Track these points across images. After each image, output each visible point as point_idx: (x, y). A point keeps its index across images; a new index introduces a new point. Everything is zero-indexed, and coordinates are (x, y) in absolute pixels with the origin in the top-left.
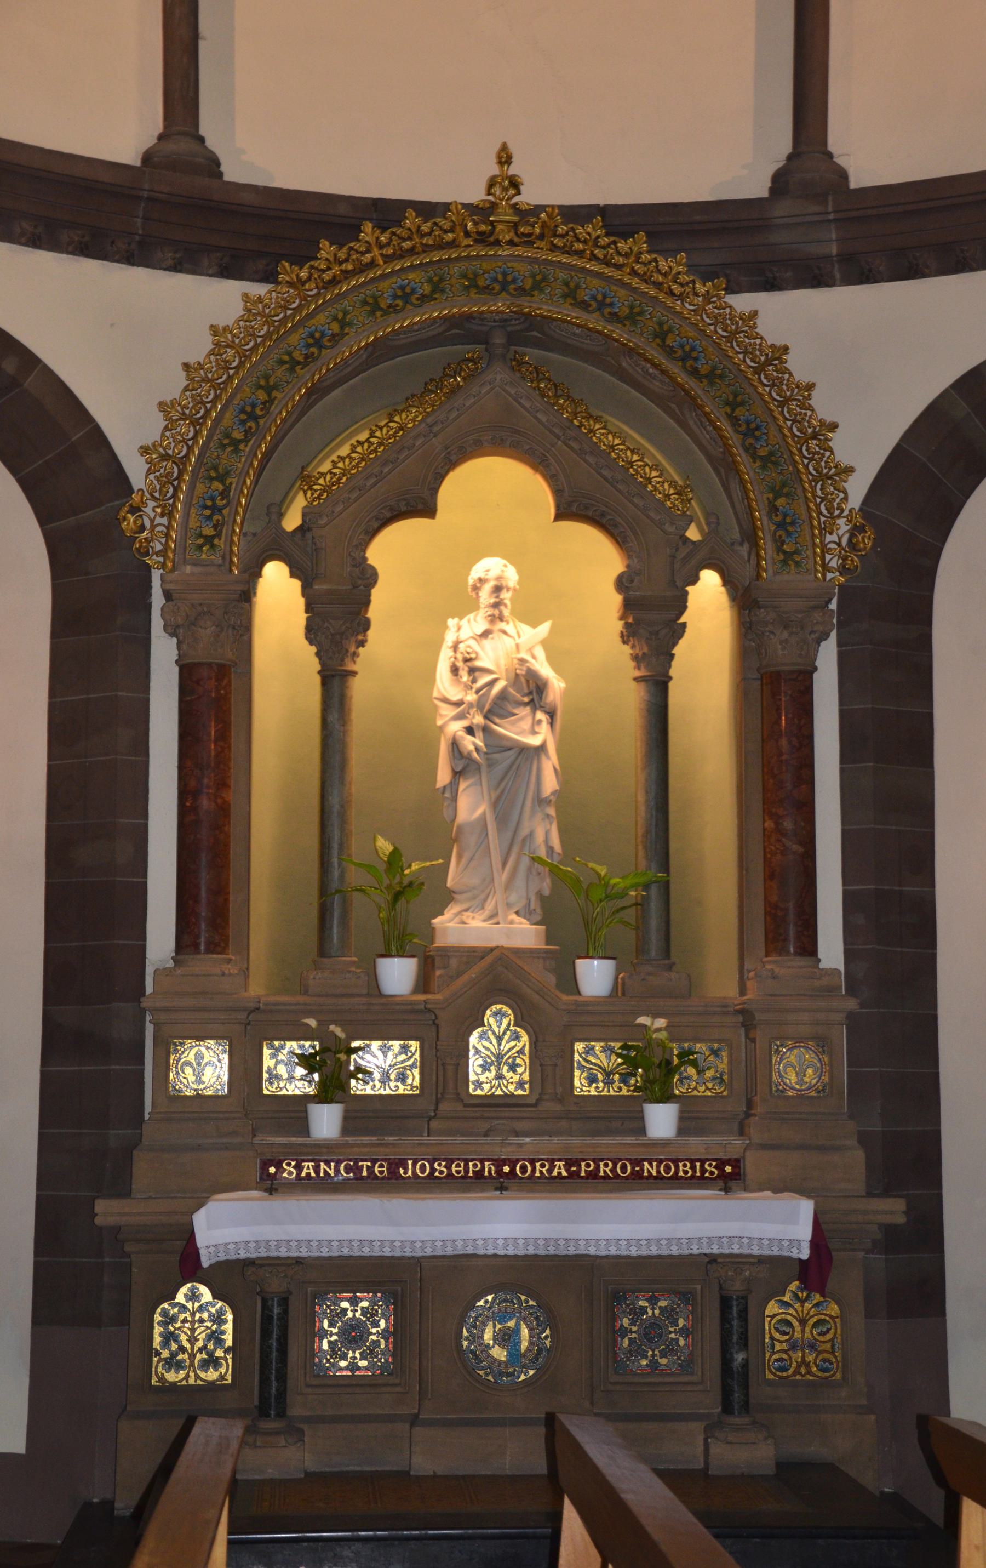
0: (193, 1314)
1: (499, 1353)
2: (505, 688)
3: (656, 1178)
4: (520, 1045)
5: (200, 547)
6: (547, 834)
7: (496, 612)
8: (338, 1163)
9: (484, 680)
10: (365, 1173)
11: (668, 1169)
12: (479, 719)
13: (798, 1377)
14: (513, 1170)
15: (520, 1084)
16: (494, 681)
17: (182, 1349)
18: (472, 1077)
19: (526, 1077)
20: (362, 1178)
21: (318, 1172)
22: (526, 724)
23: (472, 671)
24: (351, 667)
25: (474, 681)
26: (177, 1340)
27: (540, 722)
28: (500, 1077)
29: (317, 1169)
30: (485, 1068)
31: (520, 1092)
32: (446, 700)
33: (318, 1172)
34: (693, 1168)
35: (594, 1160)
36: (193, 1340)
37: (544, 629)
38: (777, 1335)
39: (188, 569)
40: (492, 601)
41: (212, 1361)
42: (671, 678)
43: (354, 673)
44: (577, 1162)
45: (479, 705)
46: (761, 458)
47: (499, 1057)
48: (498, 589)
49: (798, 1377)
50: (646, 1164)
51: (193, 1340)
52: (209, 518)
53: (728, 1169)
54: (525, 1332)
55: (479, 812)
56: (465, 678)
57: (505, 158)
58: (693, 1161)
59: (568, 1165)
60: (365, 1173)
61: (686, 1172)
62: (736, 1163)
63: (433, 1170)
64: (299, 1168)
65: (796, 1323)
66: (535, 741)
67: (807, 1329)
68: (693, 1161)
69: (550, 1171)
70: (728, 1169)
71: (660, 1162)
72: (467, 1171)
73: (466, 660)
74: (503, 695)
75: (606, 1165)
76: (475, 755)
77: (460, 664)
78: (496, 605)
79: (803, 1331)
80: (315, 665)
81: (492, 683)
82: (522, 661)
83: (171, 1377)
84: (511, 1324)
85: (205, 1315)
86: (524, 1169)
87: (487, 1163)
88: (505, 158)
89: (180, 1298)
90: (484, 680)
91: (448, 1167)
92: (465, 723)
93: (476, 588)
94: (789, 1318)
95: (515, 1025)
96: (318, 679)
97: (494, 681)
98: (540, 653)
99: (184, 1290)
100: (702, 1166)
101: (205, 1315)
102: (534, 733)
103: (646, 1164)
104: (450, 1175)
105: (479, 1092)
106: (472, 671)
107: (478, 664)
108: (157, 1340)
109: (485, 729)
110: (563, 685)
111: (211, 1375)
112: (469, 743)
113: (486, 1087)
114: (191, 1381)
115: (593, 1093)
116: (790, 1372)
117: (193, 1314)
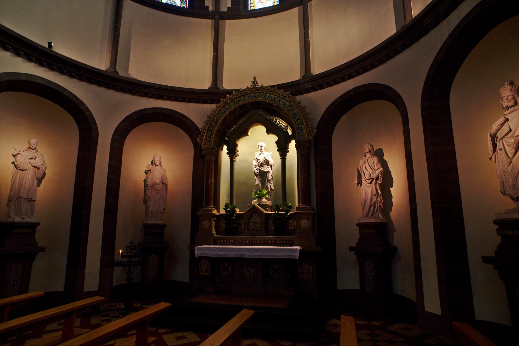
0: (204, 264)
1: (248, 274)
2: (262, 162)
3: (279, 243)
4: (259, 221)
5: (208, 142)
6: (270, 186)
7: (261, 150)
8: (226, 240)
9: (259, 161)
10: (231, 242)
11: (281, 242)
12: (258, 167)
13: (304, 279)
14: (254, 242)
15: (259, 227)
16: (261, 161)
17: (203, 269)
18: (251, 226)
19: (260, 226)
20: (230, 243)
21: (223, 242)
22: (266, 168)
23: (257, 160)
24: (234, 160)
25: (258, 161)
26: (202, 268)
27: (268, 167)
28: (255, 226)
29: (223, 241)
30: (253, 224)
31: (259, 229)
32: (254, 165)
33: (223, 242)
34: (285, 242)
35: (268, 240)
36: (204, 268)
37: (271, 153)
38: (300, 271)
39: (206, 146)
40: (261, 148)
41: (207, 272)
42: (286, 158)
43: (236, 161)
44: (265, 241)
45: (258, 165)
46: (296, 119)
47: (255, 222)
48: (261, 147)
49: (304, 279)
50: (277, 241)
51: (204, 268)
52: (209, 138)
53: (292, 242)
54: (252, 270)
55: (258, 183)
56: (256, 160)
57: (255, 78)
58: (285, 241)
59: (264, 241)
60: (231, 242)
61: (284, 242)
62: (293, 241)
63: (241, 242)
64: (220, 241)
65: (304, 269)
66: (267, 171)
67: (306, 270)
68: (285, 241)
69: (261, 242)
70: (292, 242)
71: (279, 241)
72: (247, 242)
73: (257, 158)
74: (262, 163)
75: (270, 241)
76: (257, 173)
77: (256, 159)
78: (261, 149)
79: (305, 271)
80: (229, 160)
81: (260, 162)
82: (265, 158)
83: (201, 274)
84: (250, 269)
85: (206, 264)
86: (256, 242)
87: (250, 241)
88: (255, 78)
89: (203, 262)
90: (259, 161)
91: (244, 241)
92: (256, 168)
93: (258, 147)
94: (302, 268)
95: (258, 217)
96: (230, 162)
97: (261, 161)
98: (270, 157)
99: (203, 260)
100: (287, 242)
101: (206, 264)
102: (267, 169)
103: (277, 241)
104: (244, 243)
105: (252, 228)
106: (257, 160)
107: (258, 159)
108: (199, 268)
109: (259, 169)
110: (273, 162)
111: (207, 274)
112: (256, 171)
113: (253, 228)
114: (204, 275)
115: (272, 228)
116: (303, 278)
117: (204, 264)
